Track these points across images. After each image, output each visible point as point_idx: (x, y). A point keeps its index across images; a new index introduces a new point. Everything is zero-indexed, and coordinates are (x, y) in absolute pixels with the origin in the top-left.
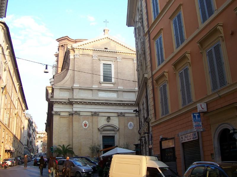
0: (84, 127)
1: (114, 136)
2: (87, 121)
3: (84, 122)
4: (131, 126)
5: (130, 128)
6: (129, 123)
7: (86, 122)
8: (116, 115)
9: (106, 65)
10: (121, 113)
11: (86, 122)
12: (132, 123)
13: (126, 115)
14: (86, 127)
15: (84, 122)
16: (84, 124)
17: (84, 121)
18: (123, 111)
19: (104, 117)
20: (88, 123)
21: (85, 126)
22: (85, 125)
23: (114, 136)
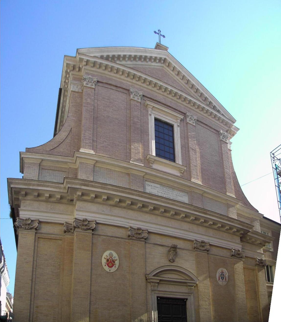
0: (107, 268)
2: (117, 253)
3: (106, 254)
4: (222, 278)
5: (220, 283)
6: (220, 270)
7: (111, 255)
8: (188, 246)
9: (161, 124)
10: (203, 242)
11: (111, 255)
12: (225, 270)
13: (214, 251)
14: (113, 269)
15: (106, 254)
16: (108, 260)
17: (104, 252)
18: (206, 239)
19: (160, 248)
20: (117, 258)
21: (110, 265)
22: (111, 263)
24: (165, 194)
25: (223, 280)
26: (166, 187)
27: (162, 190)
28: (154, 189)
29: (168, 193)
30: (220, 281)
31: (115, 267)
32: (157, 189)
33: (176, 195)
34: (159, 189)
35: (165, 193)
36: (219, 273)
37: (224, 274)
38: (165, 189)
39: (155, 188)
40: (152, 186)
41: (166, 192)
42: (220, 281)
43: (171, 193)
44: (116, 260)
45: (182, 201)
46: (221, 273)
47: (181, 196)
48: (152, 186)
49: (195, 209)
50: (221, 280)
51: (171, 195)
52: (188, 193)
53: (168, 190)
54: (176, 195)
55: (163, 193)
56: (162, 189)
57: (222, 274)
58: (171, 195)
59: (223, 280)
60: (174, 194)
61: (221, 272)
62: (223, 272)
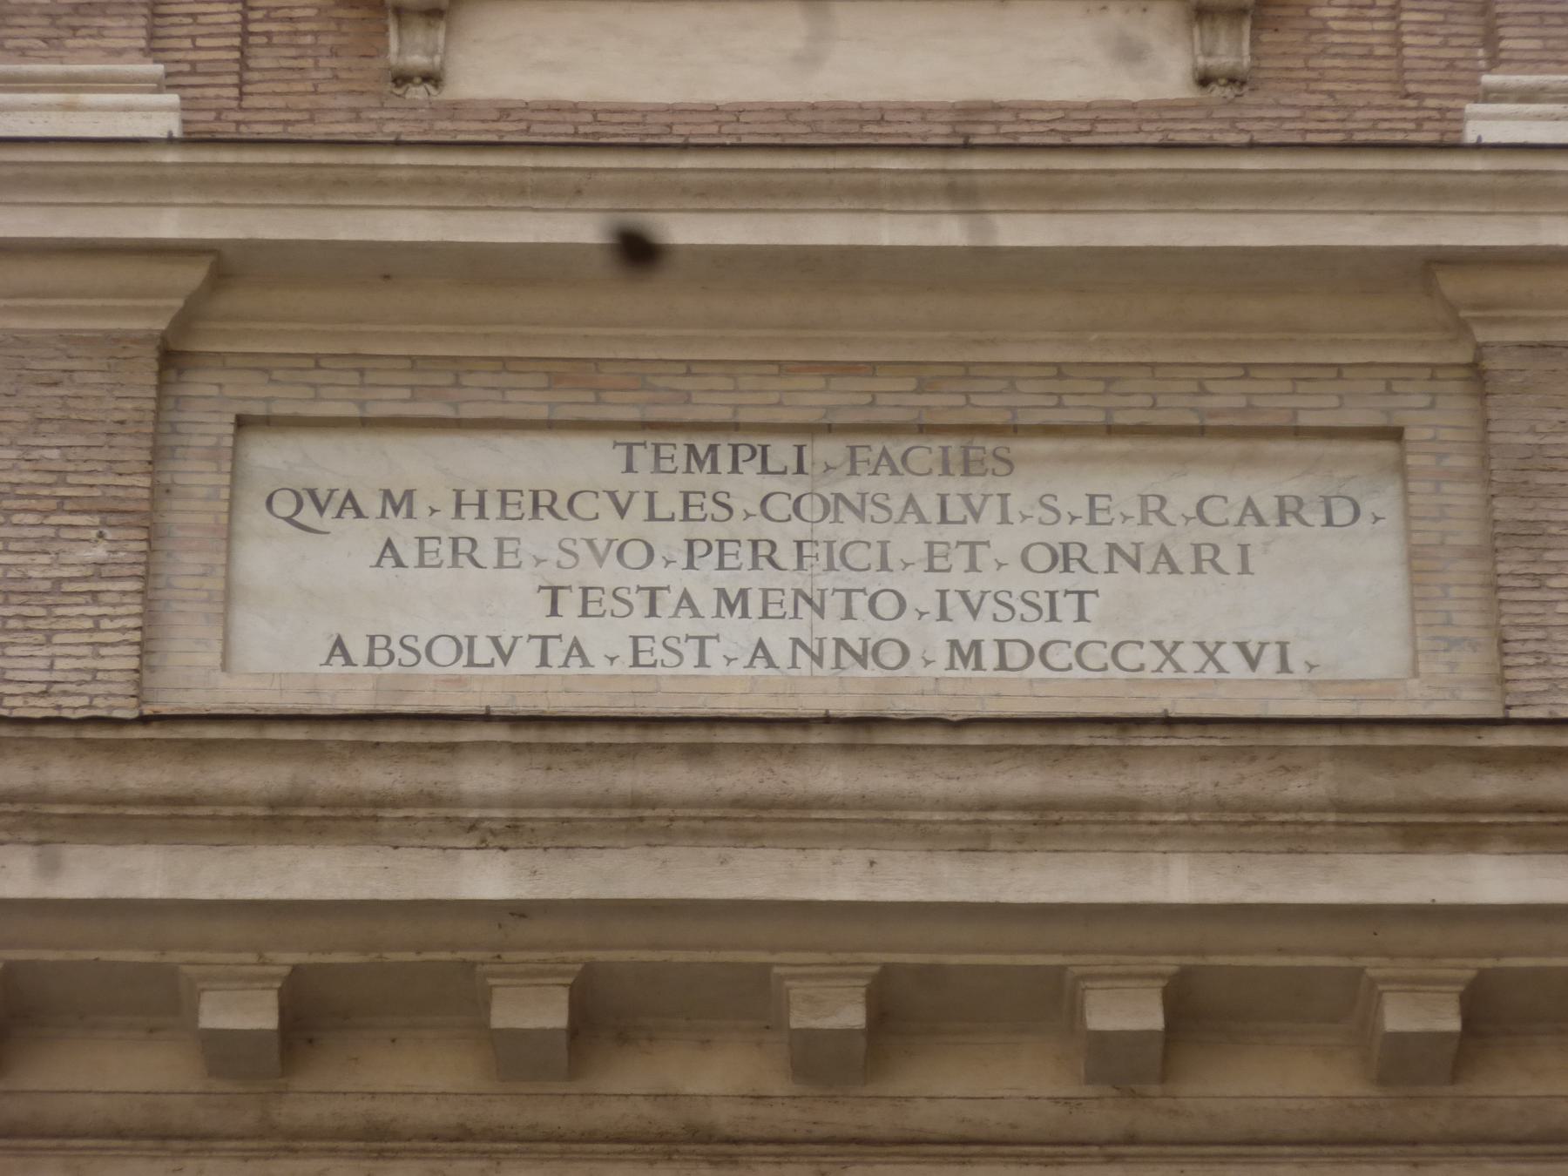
24: (735, 602)
26: (782, 451)
27: (670, 537)
28: (463, 552)
29: (838, 557)
32: (541, 536)
33: (1062, 558)
34: (609, 526)
38: (746, 486)
39: (486, 532)
41: (763, 553)
43: (909, 541)
45: (1168, 652)
47: (1205, 559)
48: (399, 502)
49: (1381, 786)
51: (921, 590)
52: (1394, 434)
53: (833, 506)
54: (1062, 558)
55: (704, 583)
58: (921, 590)
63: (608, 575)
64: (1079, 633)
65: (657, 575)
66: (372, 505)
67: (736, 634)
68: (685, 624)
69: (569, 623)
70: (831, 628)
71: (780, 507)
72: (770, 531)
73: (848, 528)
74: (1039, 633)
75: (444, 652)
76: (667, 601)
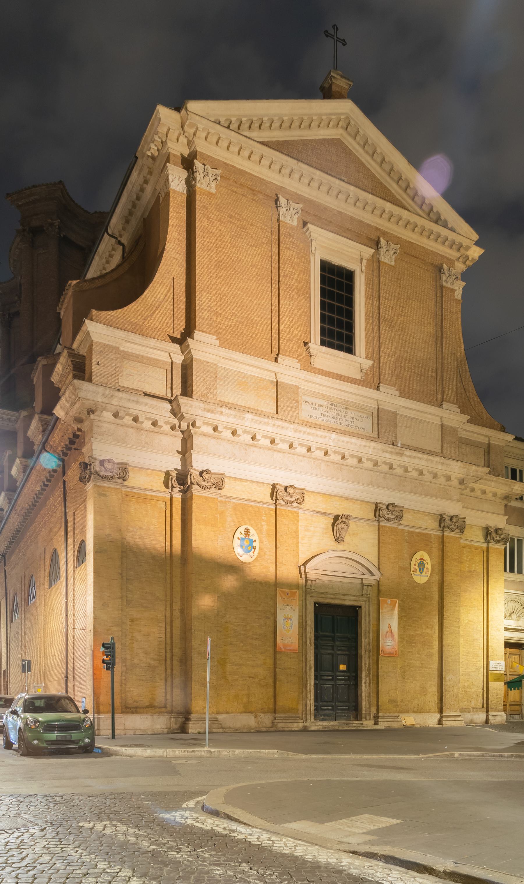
1: (360, 607)
2: (256, 530)
4: (421, 570)
6: (418, 556)
12: (426, 557)
23: (360, 607)
24: (333, 417)
25: (421, 573)
27: (329, 411)
28: (316, 409)
30: (417, 575)
31: (253, 553)
32: (321, 409)
33: (352, 418)
35: (334, 416)
36: (417, 560)
37: (425, 562)
39: (317, 407)
40: (312, 404)
42: (417, 575)
44: (255, 541)
46: (419, 561)
50: (418, 573)
51: (344, 419)
55: (331, 415)
56: (329, 408)
57: (421, 562)
58: (344, 419)
59: (421, 573)
60: (349, 416)
61: (420, 559)
62: (424, 560)
63: (325, 413)
64: (353, 425)
65: (328, 414)
66: (310, 403)
67: (333, 420)
68: (330, 419)
69: (322, 417)
70: (339, 421)
71: (335, 410)
72: (335, 412)
73: (339, 413)
74: (351, 424)
75: (315, 417)
76: (329, 416)
